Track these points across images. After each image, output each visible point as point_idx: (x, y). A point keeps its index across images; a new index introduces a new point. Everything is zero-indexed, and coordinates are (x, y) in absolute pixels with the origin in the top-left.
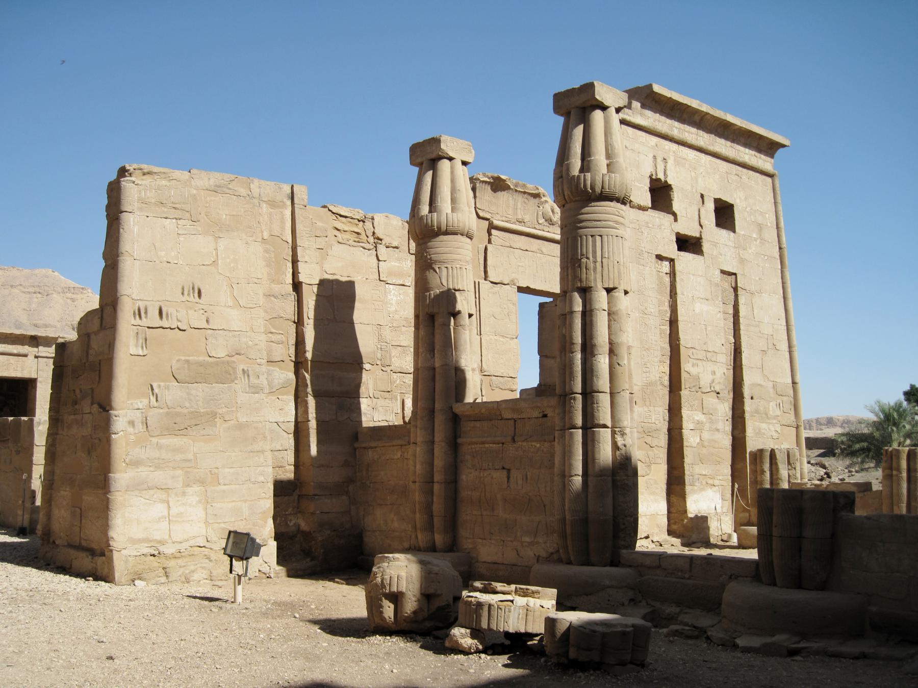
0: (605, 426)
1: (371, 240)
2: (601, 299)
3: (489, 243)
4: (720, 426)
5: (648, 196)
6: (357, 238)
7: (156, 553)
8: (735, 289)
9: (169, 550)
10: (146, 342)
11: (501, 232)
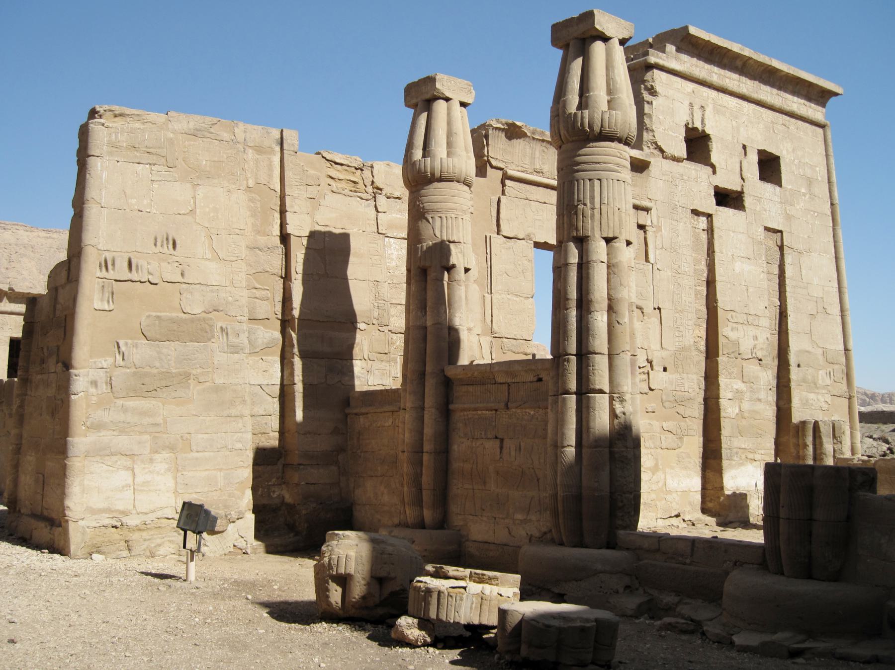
0: (601, 392)
1: (370, 189)
2: (599, 250)
3: (502, 195)
4: (762, 395)
5: (683, 146)
6: (354, 187)
7: (118, 524)
8: (781, 248)
9: (133, 521)
10: (113, 297)
11: (516, 183)
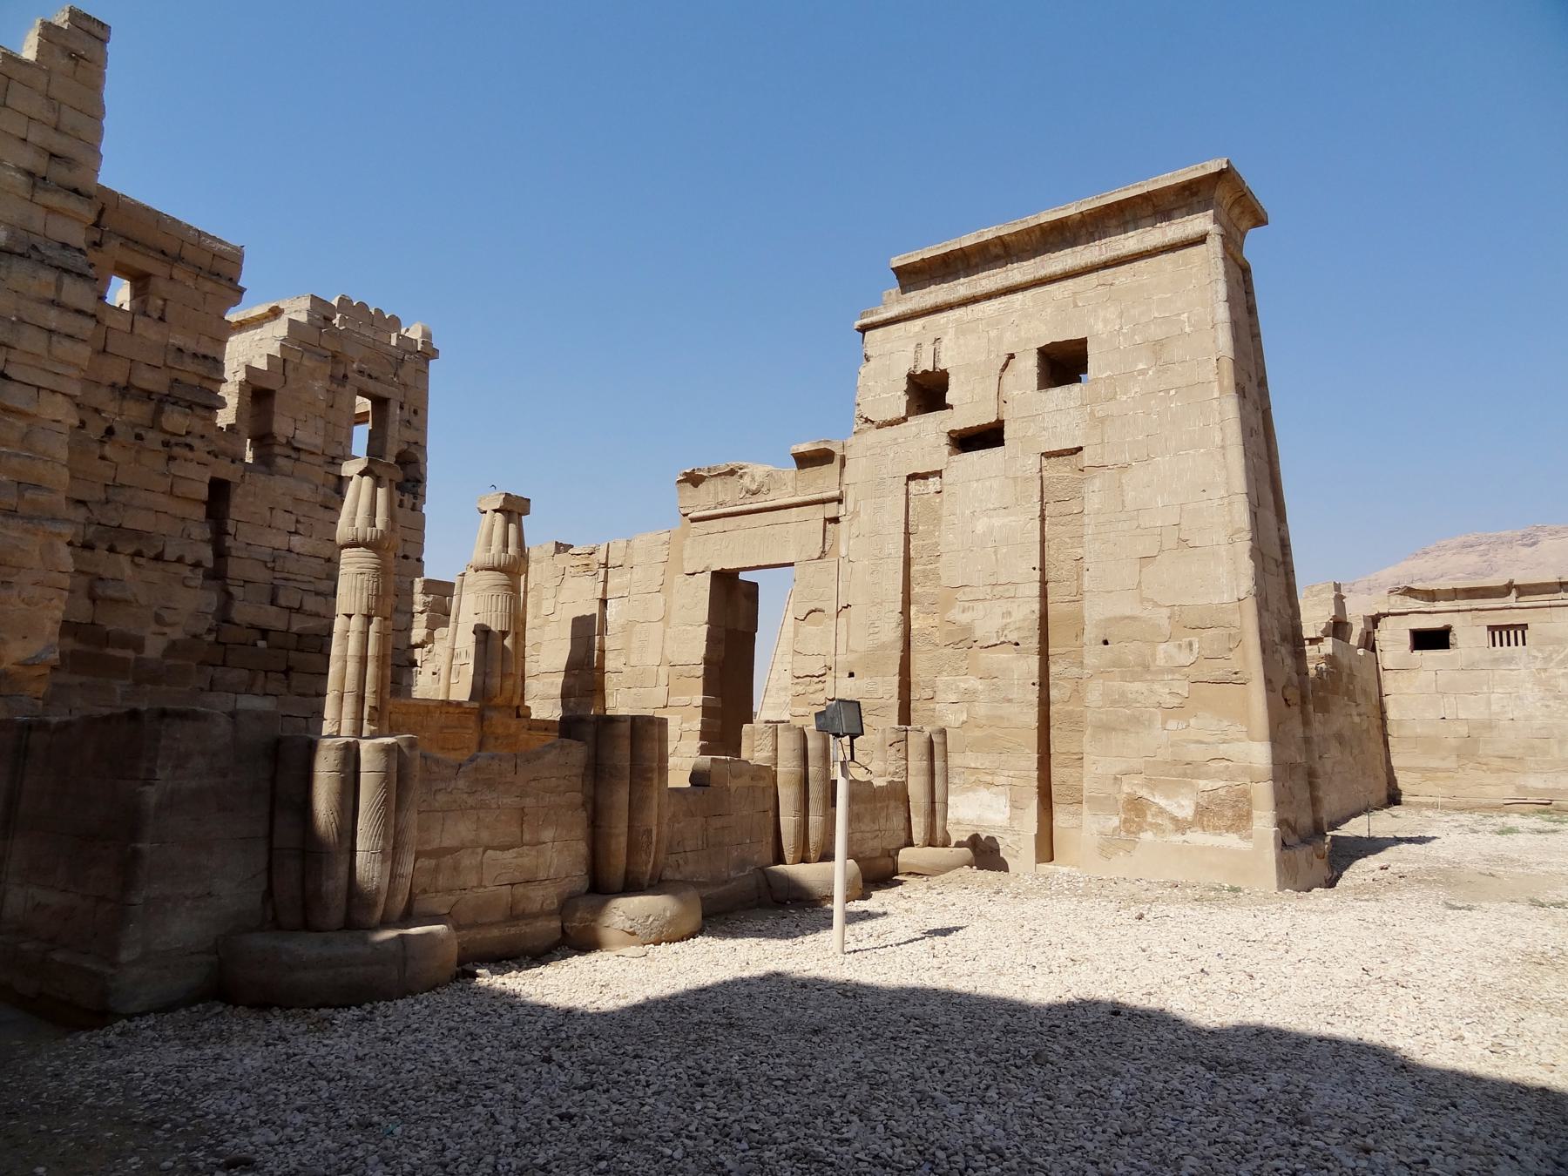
4: (1015, 694)
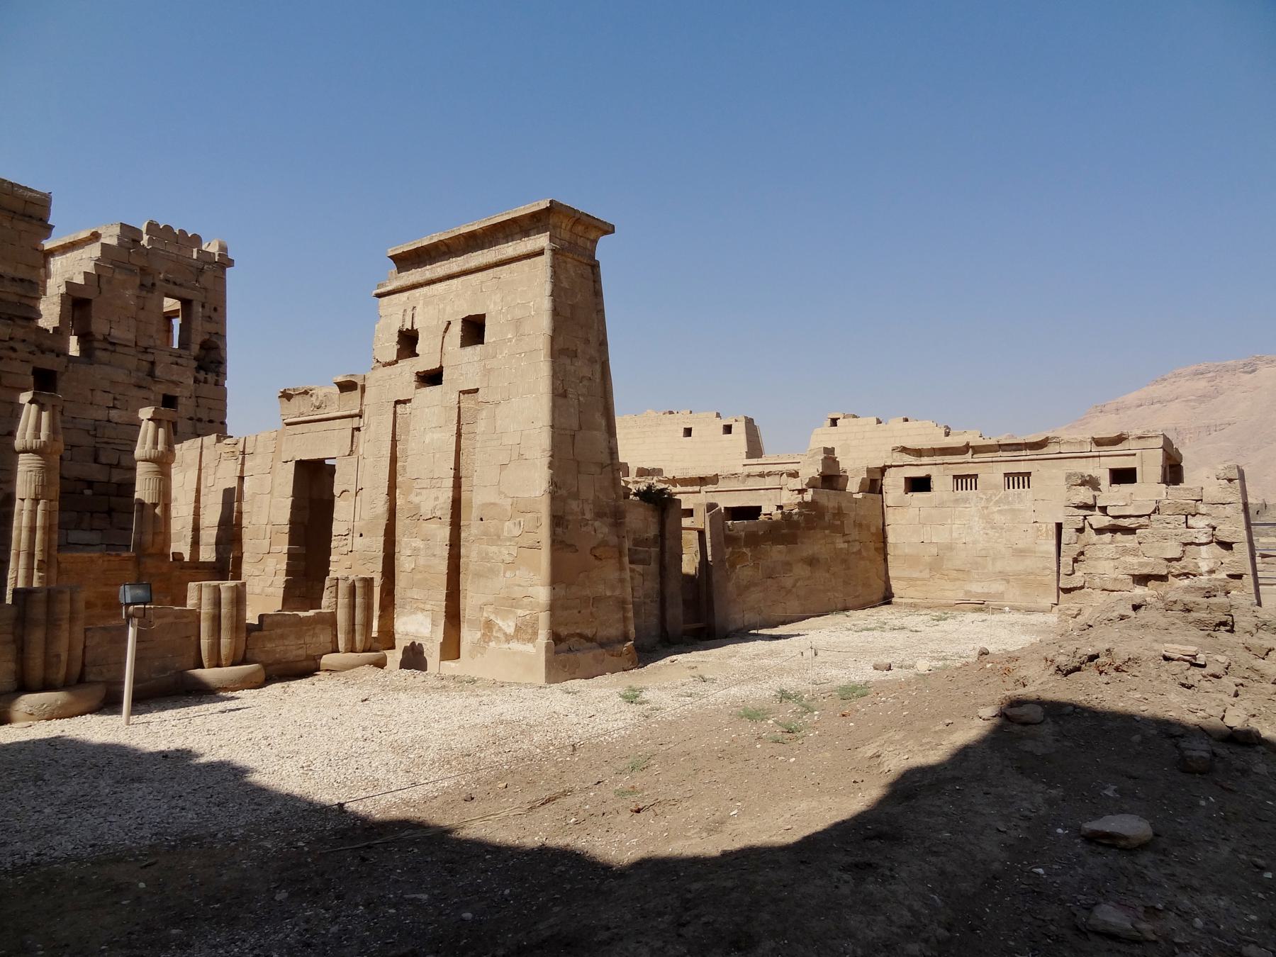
4: (438, 552)
